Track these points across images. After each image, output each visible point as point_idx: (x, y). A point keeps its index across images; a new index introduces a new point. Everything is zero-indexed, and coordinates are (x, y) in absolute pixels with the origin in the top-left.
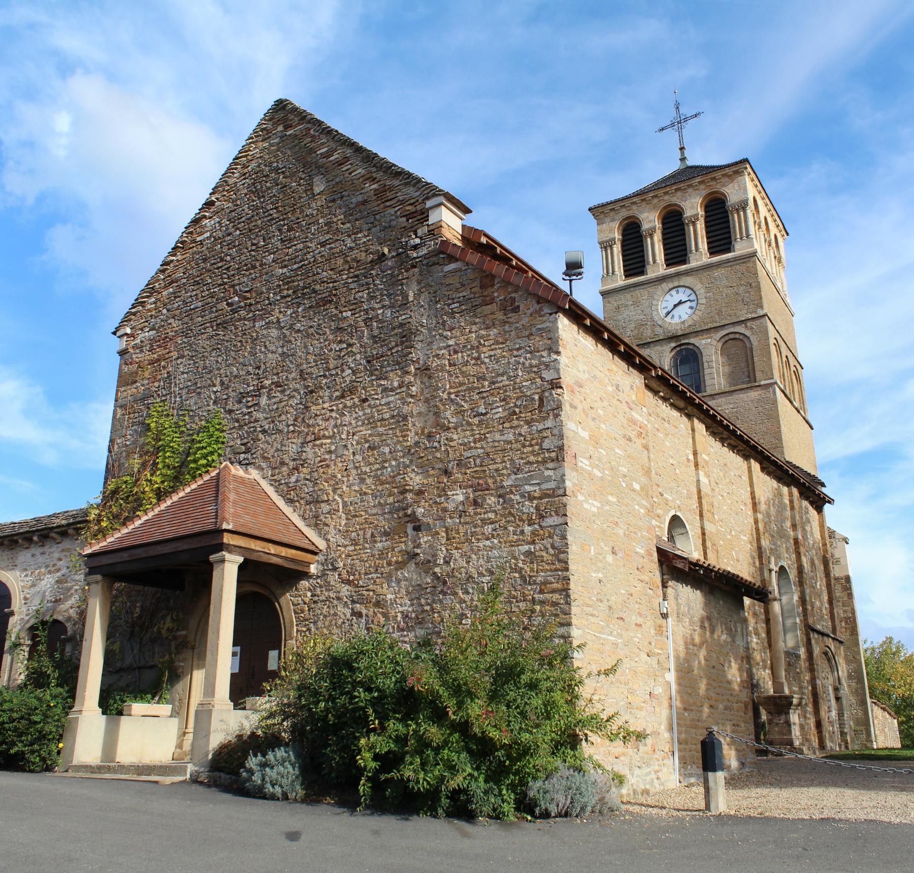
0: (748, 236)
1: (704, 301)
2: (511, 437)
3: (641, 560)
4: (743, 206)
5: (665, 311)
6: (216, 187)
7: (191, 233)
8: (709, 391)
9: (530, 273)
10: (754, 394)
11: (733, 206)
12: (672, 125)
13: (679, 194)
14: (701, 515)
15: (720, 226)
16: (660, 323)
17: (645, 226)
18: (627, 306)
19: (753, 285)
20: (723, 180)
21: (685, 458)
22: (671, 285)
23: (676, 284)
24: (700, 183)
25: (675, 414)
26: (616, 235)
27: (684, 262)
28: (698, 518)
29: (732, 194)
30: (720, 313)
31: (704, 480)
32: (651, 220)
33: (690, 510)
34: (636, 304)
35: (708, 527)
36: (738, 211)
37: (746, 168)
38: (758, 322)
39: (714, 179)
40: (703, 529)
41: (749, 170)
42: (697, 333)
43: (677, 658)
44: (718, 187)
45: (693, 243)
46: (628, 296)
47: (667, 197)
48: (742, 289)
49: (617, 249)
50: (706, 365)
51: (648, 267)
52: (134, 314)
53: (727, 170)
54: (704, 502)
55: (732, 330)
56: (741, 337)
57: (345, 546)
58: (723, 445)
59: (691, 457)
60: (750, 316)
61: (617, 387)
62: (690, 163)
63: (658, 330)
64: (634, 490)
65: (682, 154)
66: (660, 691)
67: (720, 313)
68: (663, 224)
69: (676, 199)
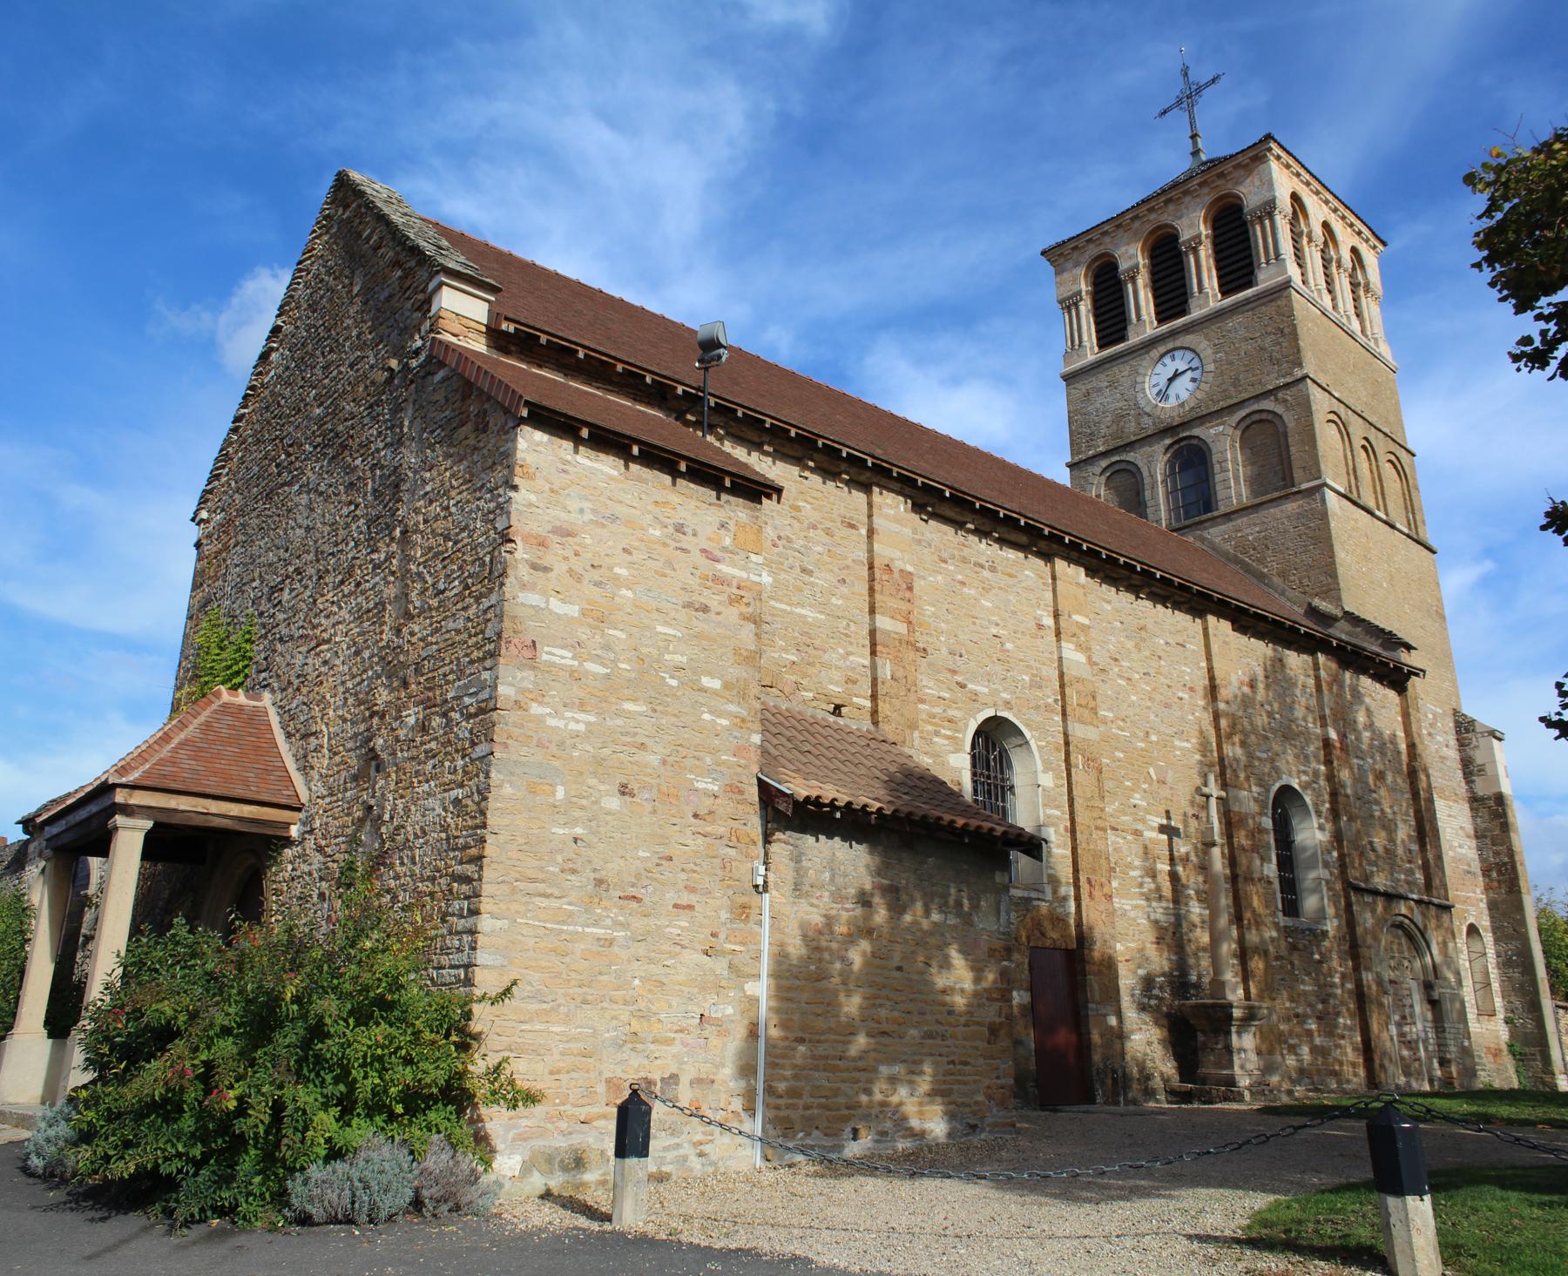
0: (1278, 255)
1: (1211, 367)
2: (460, 624)
3: (709, 802)
4: (1269, 209)
5: (1156, 390)
6: (281, 307)
7: (260, 373)
8: (1223, 509)
9: (619, 368)
10: (1291, 507)
11: (1254, 211)
12: (1179, 102)
13: (1171, 207)
14: (1064, 714)
15: (1236, 249)
16: (1147, 409)
17: (1123, 266)
18: (1100, 390)
19: (1286, 331)
20: (1235, 174)
21: (1032, 624)
22: (1162, 349)
23: (1170, 346)
24: (1201, 185)
25: (1011, 555)
26: (1083, 287)
27: (1183, 313)
28: (1058, 718)
29: (1251, 196)
30: (1236, 383)
31: (1070, 652)
32: (1133, 256)
33: (1037, 707)
34: (1113, 385)
35: (1078, 731)
36: (1261, 219)
37: (1270, 149)
38: (1294, 390)
39: (1221, 175)
40: (1066, 735)
41: (1277, 150)
42: (1202, 419)
43: (780, 957)
44: (1226, 187)
45: (1195, 281)
46: (1102, 377)
47: (1153, 216)
48: (1269, 339)
49: (1085, 307)
50: (1217, 467)
51: (1130, 328)
52: (210, 492)
53: (1240, 159)
54: (1067, 690)
55: (1256, 407)
56: (1270, 417)
57: (323, 798)
58: (1138, 597)
59: (1049, 621)
60: (1282, 381)
61: (680, 529)
62: (1204, 157)
63: (1146, 421)
64: (703, 690)
65: (1195, 144)
66: (730, 1011)
67: (1236, 383)
68: (1152, 257)
69: (1166, 218)
